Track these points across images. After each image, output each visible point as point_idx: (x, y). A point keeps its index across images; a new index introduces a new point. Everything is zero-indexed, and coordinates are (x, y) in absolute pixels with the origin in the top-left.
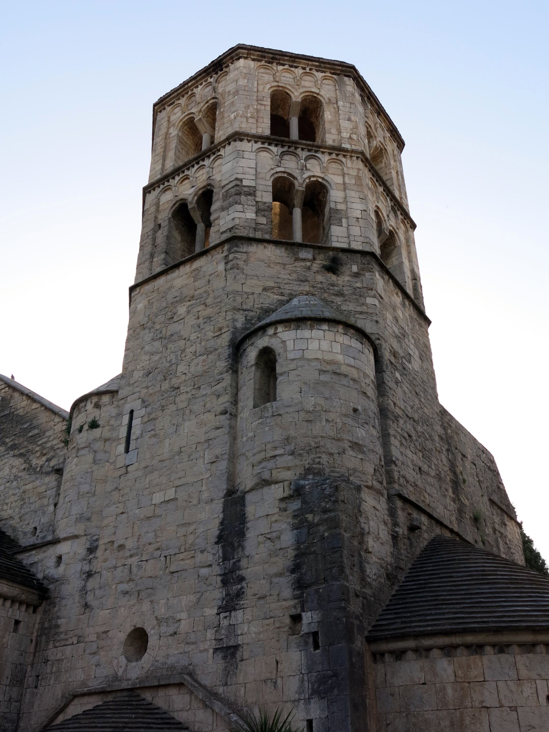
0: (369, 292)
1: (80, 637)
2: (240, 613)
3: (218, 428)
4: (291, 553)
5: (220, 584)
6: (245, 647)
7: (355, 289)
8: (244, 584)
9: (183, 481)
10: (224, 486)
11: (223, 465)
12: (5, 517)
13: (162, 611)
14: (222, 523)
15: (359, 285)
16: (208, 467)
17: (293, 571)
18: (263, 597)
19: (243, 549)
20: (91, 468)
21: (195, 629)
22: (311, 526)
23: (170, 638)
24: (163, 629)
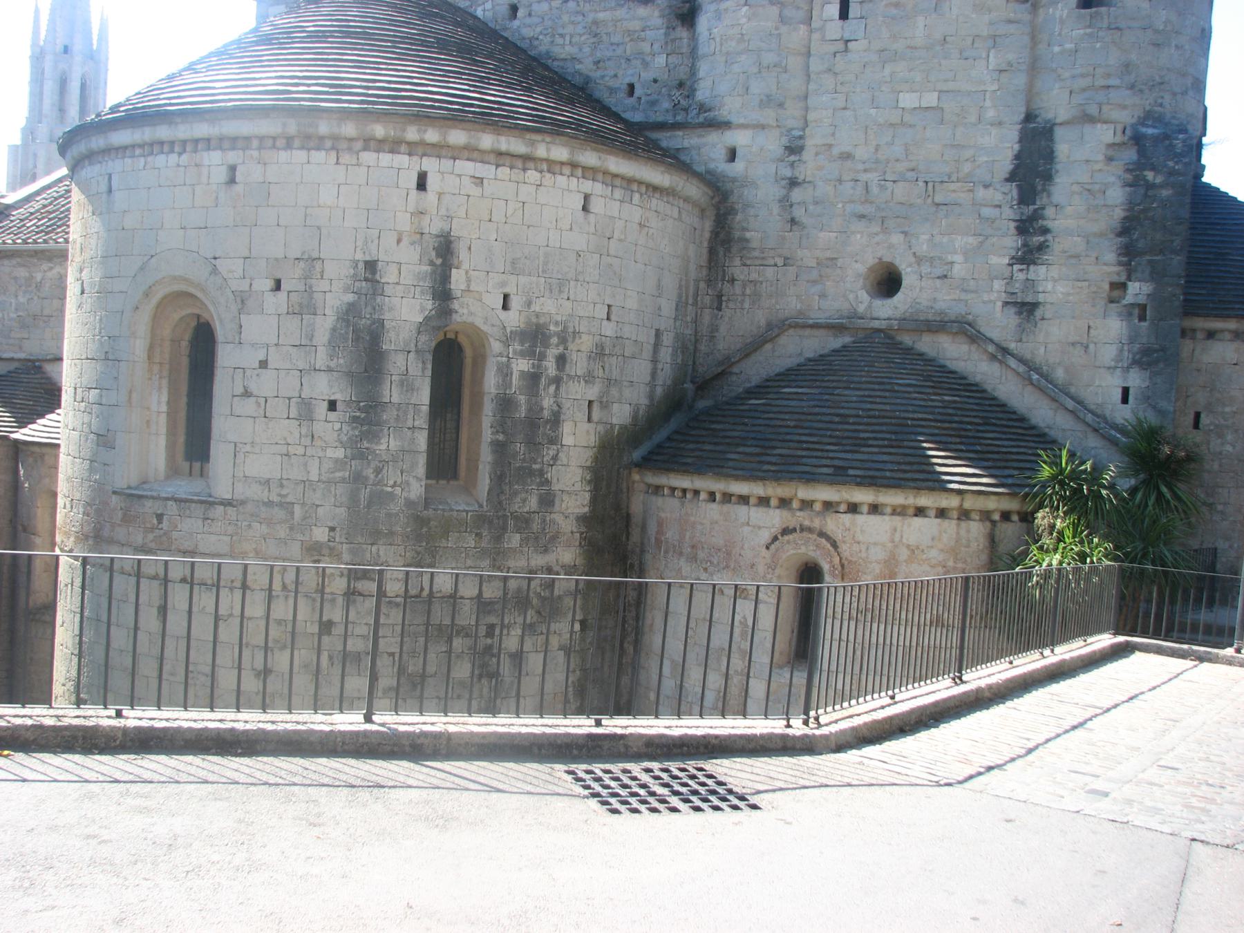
1: (786, 258)
2: (1042, 270)
3: (1010, 22)
4: (1119, 213)
5: (1013, 231)
6: (1048, 306)
8: (1049, 237)
9: (951, 86)
10: (1023, 109)
11: (1021, 80)
12: (563, 56)
13: (923, 248)
14: (1017, 157)
16: (995, 75)
17: (1119, 234)
18: (1077, 256)
19: (1049, 196)
20: (777, 29)
21: (976, 276)
22: (1150, 186)
23: (938, 282)
24: (926, 269)
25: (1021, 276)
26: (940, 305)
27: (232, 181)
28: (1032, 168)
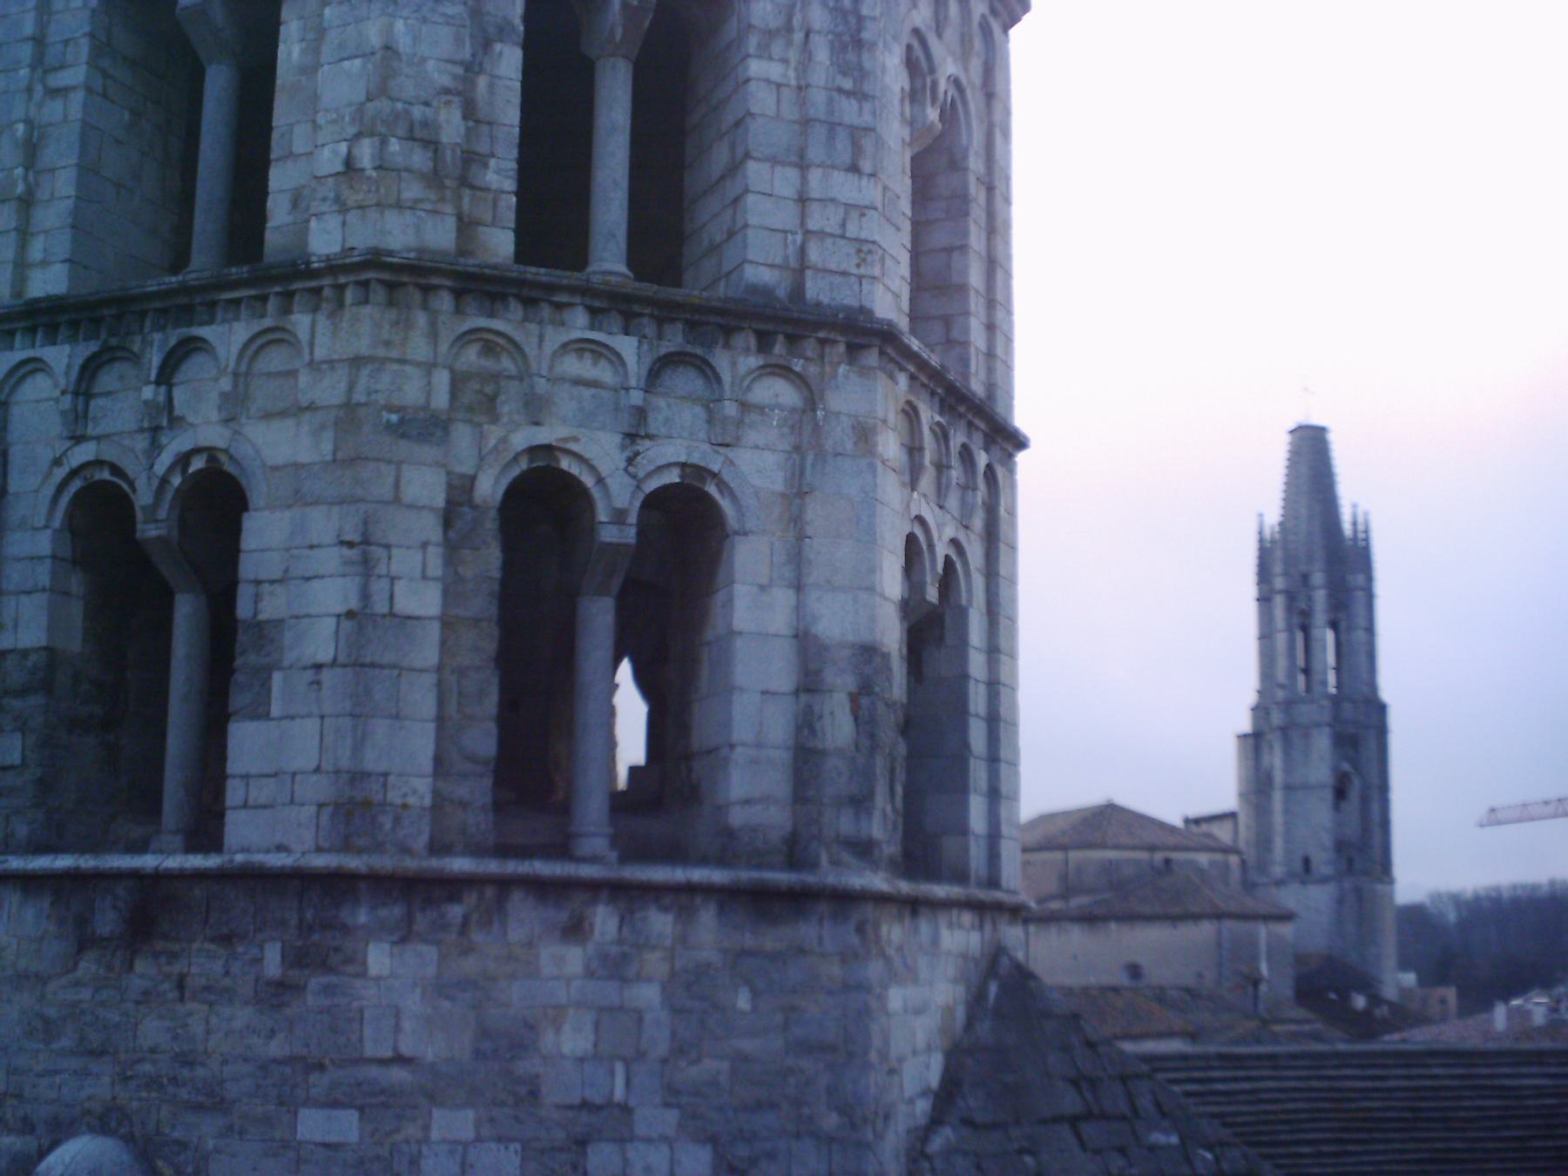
0: (314, 1077)
7: (264, 1067)
15: (276, 1048)
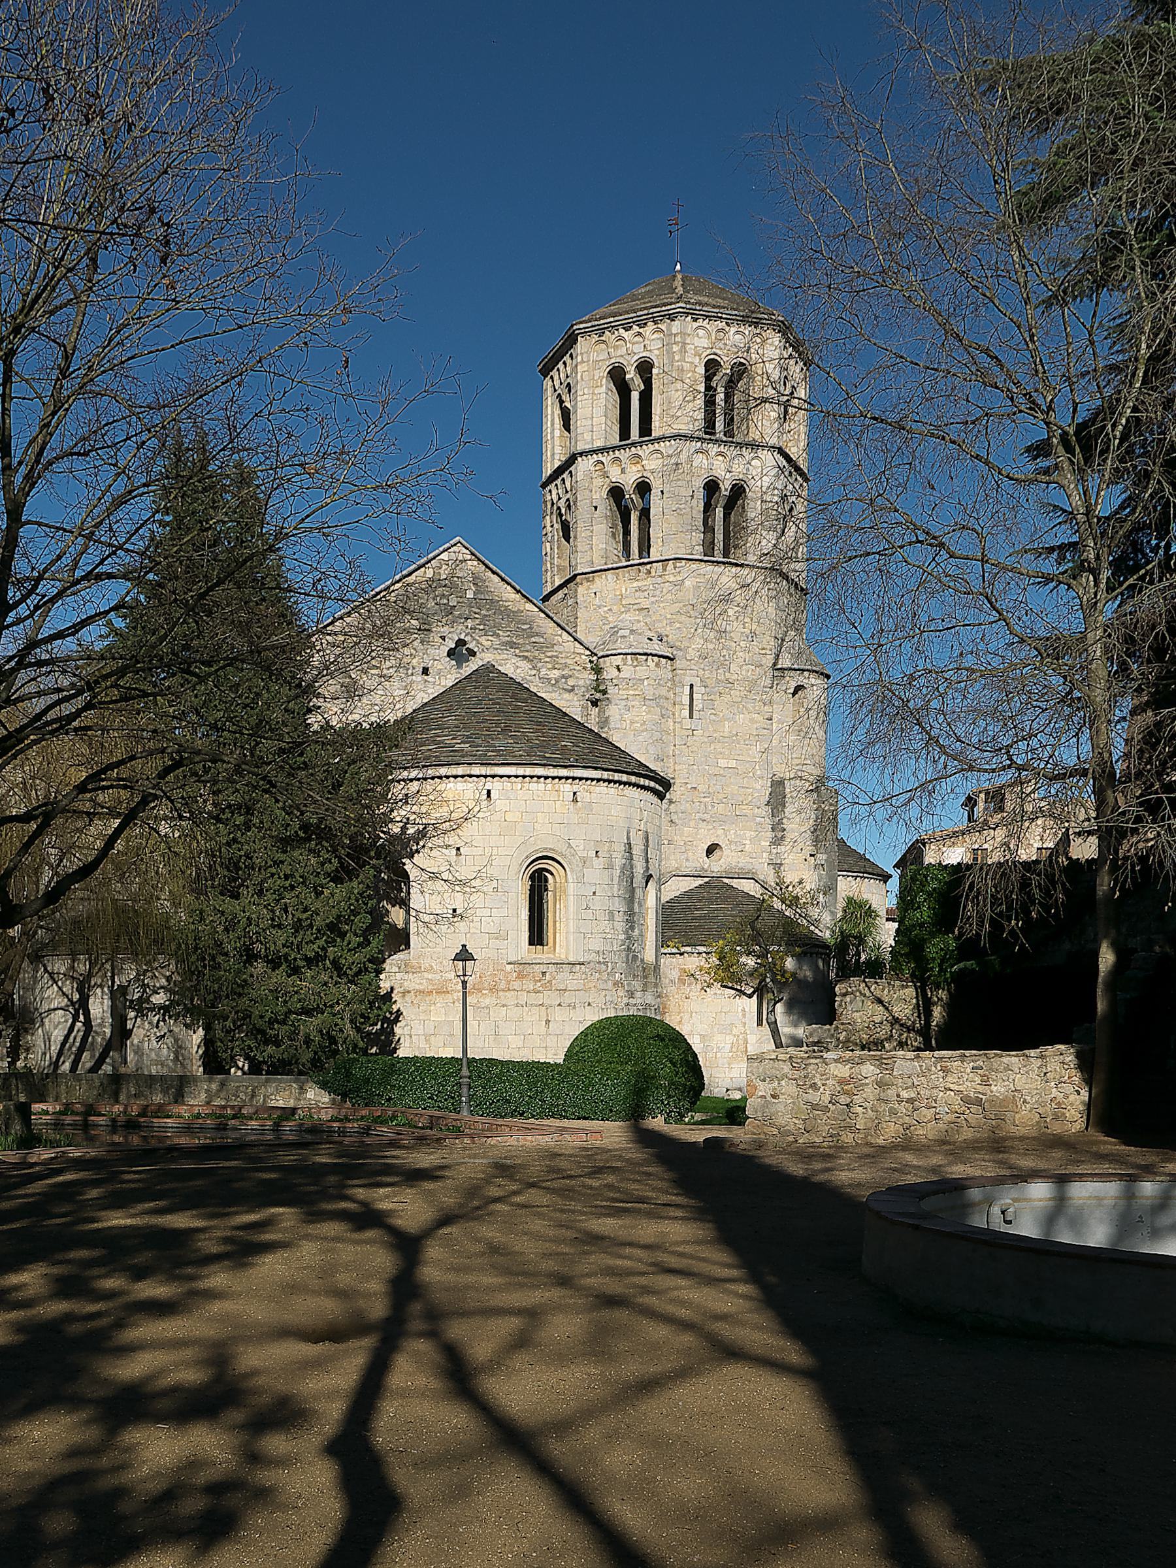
9: (741, 758)
25: (775, 851)
26: (740, 865)
27: (575, 800)
28: (777, 799)
